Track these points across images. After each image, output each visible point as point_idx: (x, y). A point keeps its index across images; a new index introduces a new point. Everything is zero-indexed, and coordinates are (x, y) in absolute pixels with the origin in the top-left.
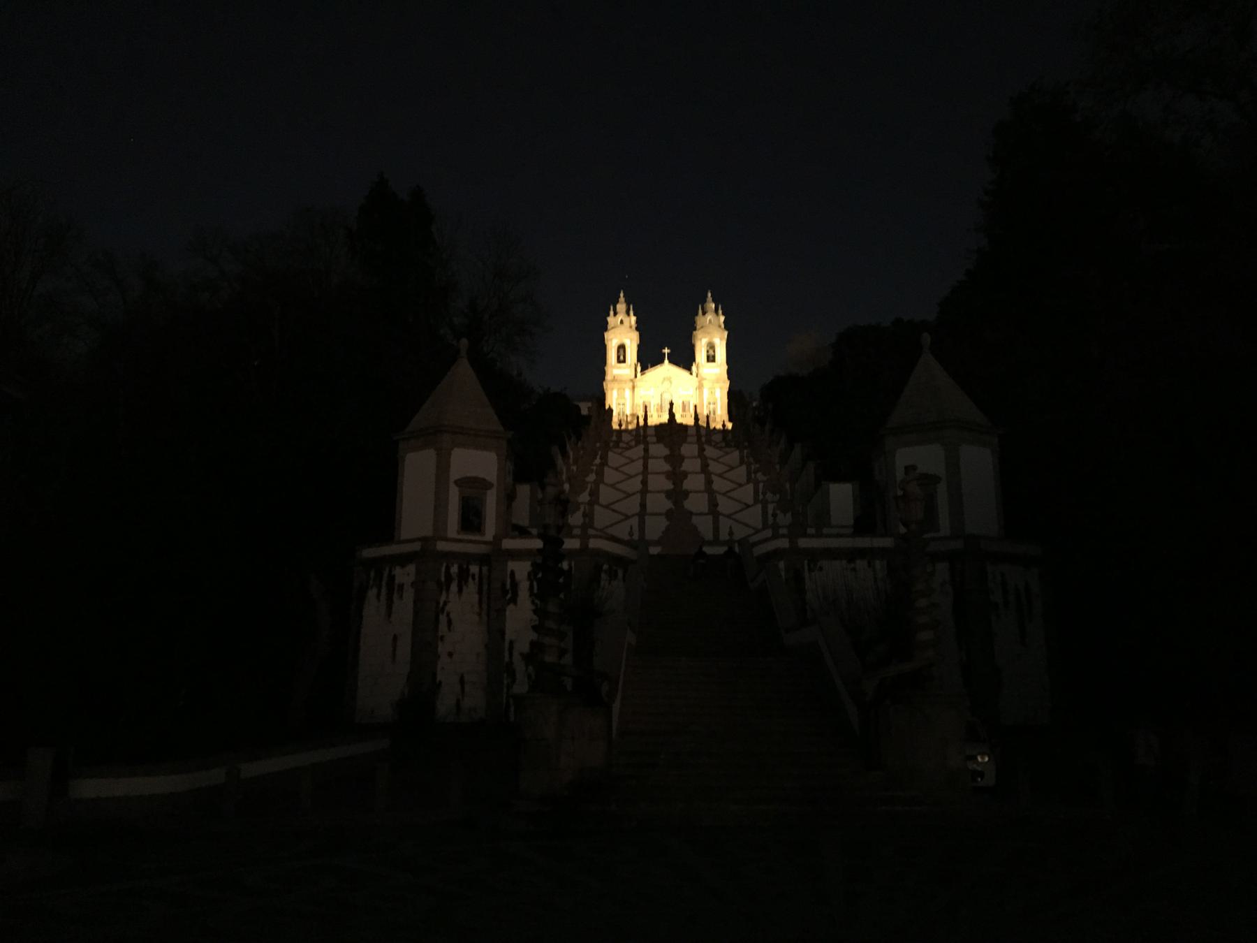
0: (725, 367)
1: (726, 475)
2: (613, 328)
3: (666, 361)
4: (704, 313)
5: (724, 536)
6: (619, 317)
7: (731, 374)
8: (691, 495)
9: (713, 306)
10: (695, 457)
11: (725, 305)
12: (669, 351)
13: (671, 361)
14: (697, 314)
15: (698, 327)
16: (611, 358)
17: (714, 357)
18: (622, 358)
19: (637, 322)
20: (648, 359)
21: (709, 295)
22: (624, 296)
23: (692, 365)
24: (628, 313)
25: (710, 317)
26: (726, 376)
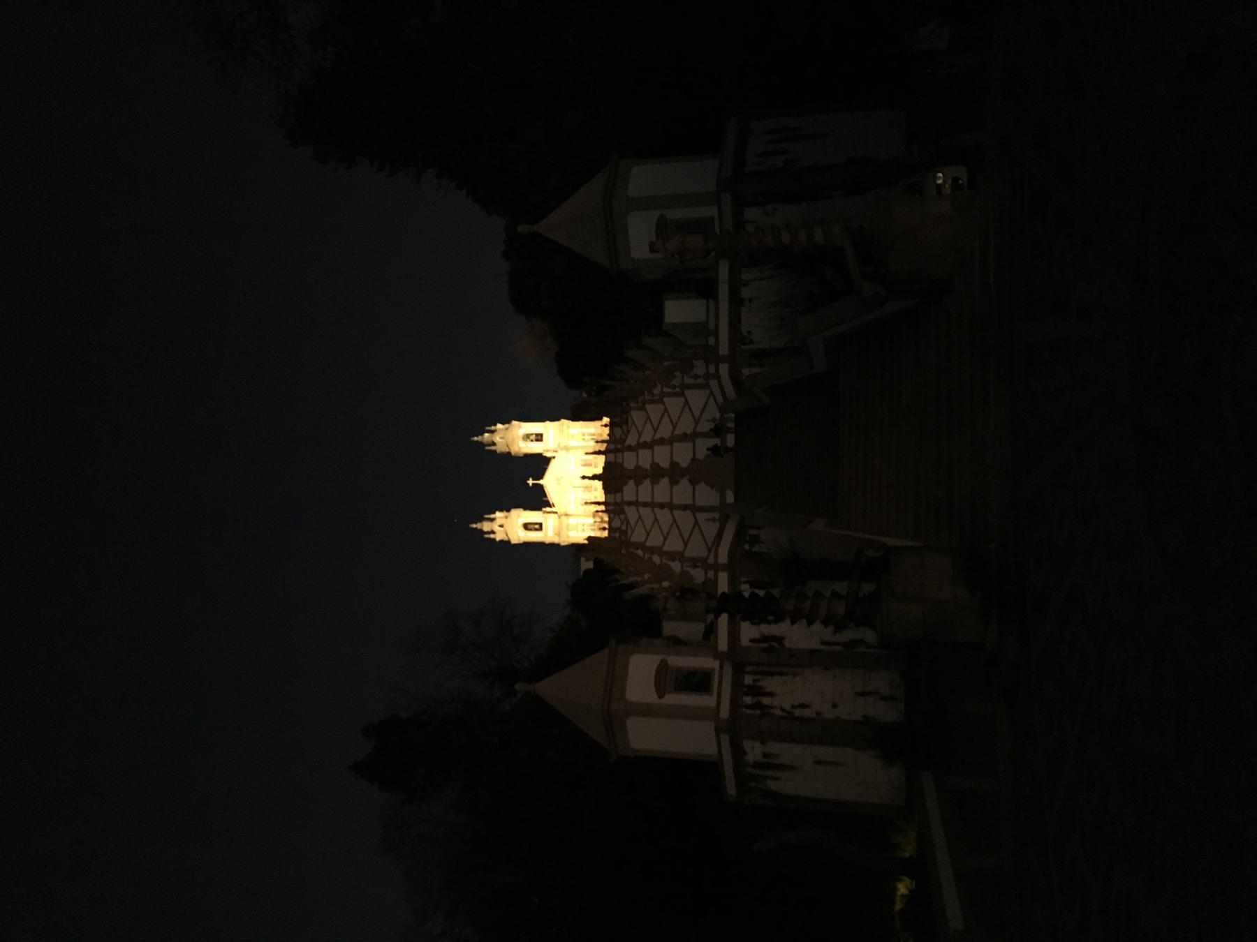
0: (548, 423)
2: (507, 535)
3: (541, 482)
4: (494, 444)
6: (496, 528)
7: (554, 418)
9: (486, 435)
12: (531, 479)
13: (541, 476)
14: (495, 451)
15: (507, 450)
17: (537, 435)
18: (537, 526)
19: (501, 510)
20: (538, 500)
21: (476, 438)
22: (476, 523)
23: (545, 457)
24: (492, 520)
25: (497, 438)
26: (556, 423)
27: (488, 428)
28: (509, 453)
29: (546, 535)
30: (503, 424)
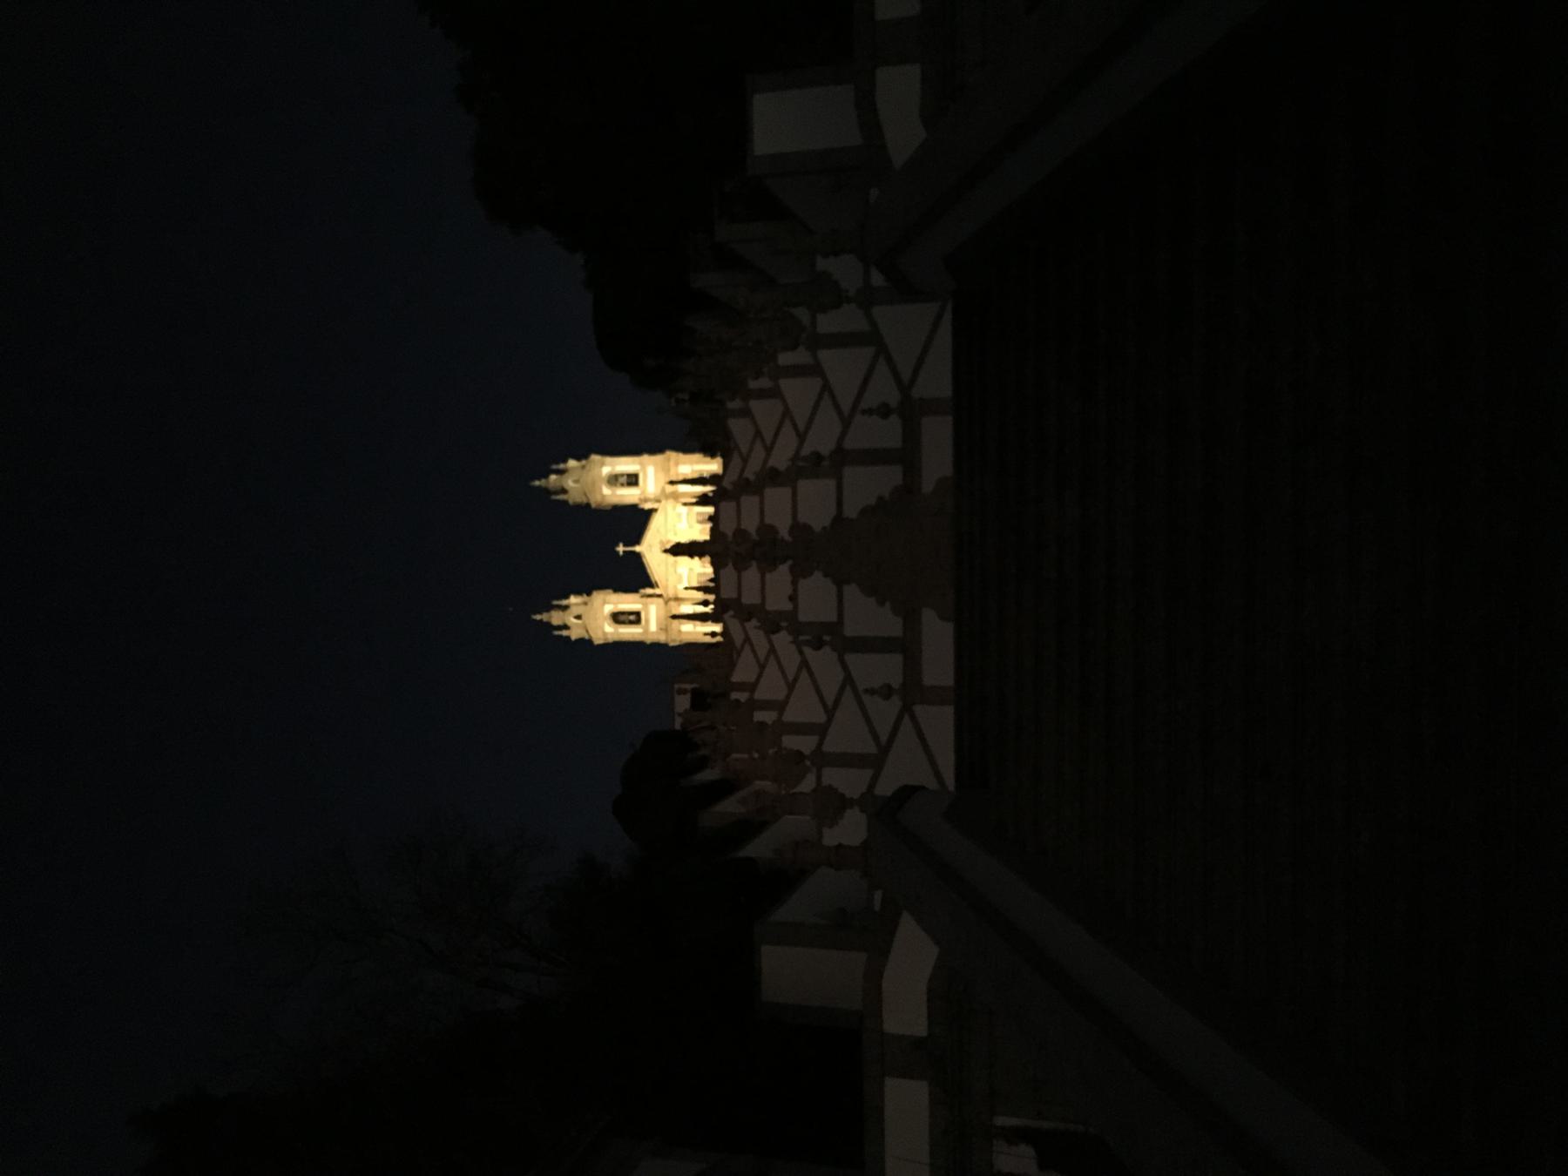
0: (646, 458)
1: (768, 439)
2: (587, 631)
3: (637, 549)
4: (564, 491)
5: (888, 434)
7: (655, 448)
8: (802, 518)
9: (553, 477)
10: (738, 505)
11: (552, 459)
12: (621, 545)
13: (637, 538)
14: (565, 502)
15: (585, 501)
16: (633, 634)
18: (632, 618)
19: (578, 593)
20: (635, 577)
21: (537, 483)
22: (540, 613)
23: (643, 510)
24: (566, 608)
25: (569, 483)
26: (659, 458)
27: (554, 467)
29: (646, 630)
30: (578, 459)
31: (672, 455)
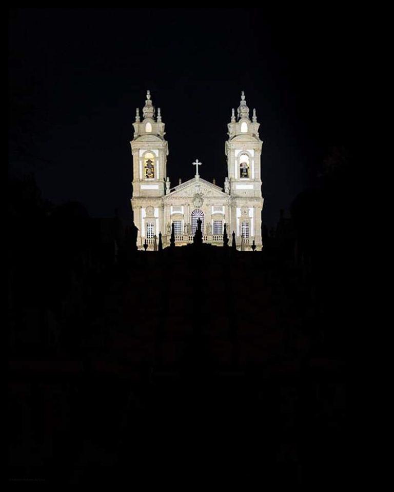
3: (197, 176)
4: (237, 120)
12: (200, 164)
19: (166, 129)
24: (155, 119)
28: (227, 138)
31: (260, 203)
